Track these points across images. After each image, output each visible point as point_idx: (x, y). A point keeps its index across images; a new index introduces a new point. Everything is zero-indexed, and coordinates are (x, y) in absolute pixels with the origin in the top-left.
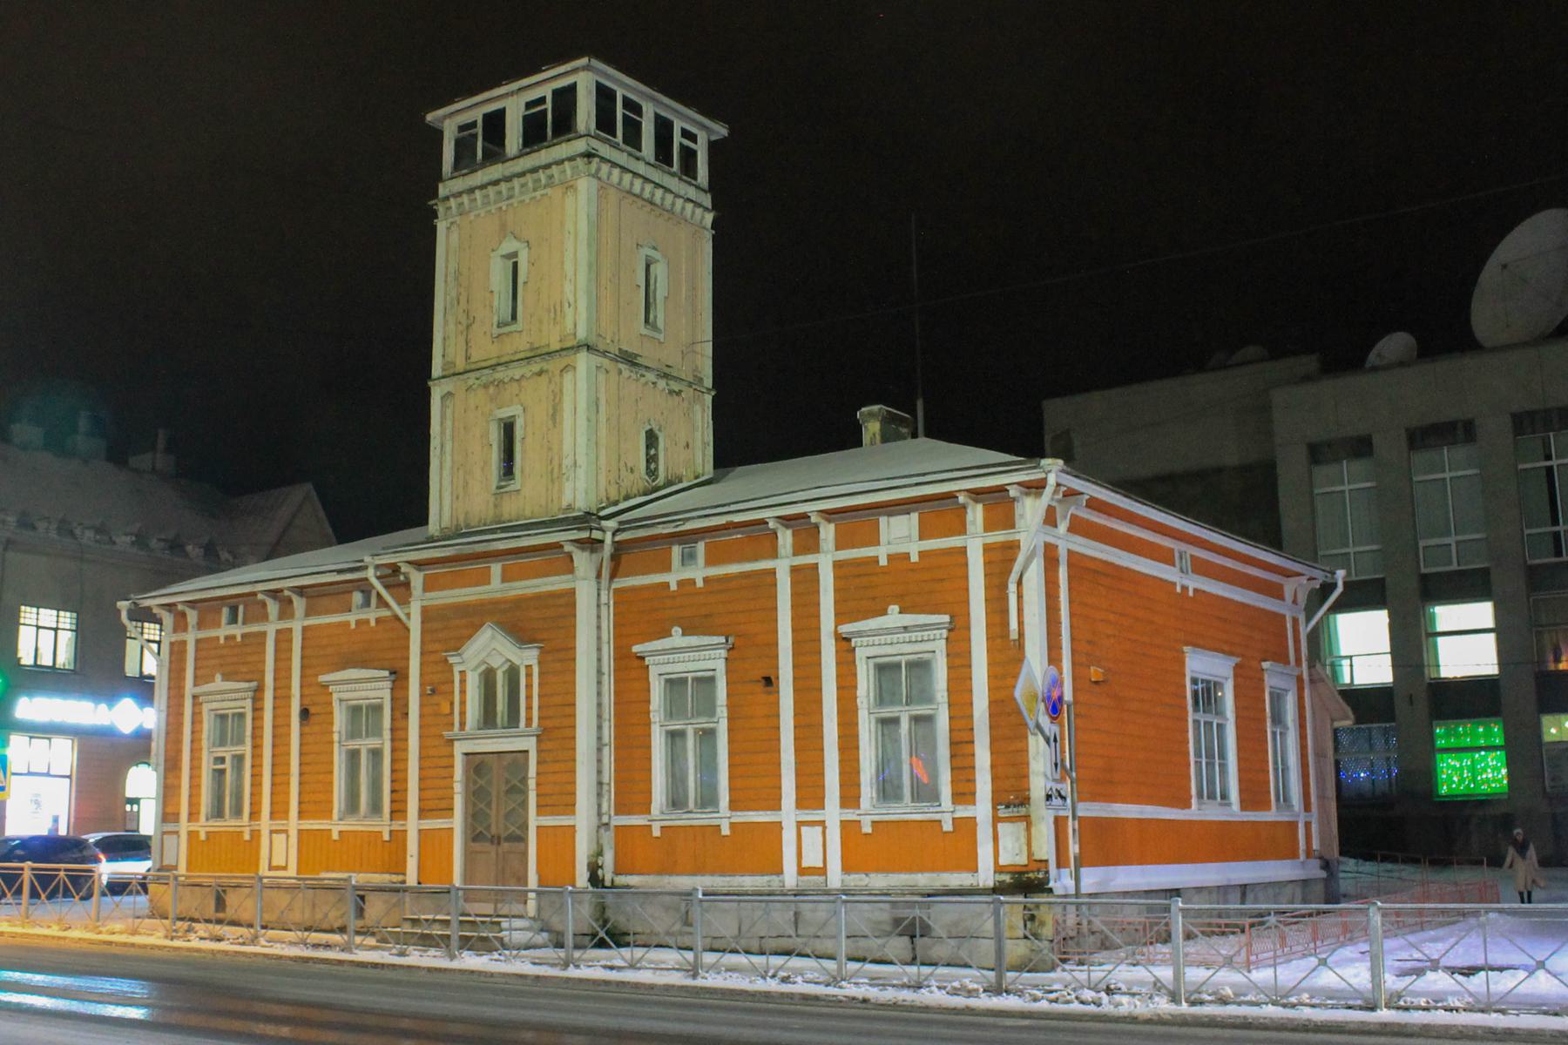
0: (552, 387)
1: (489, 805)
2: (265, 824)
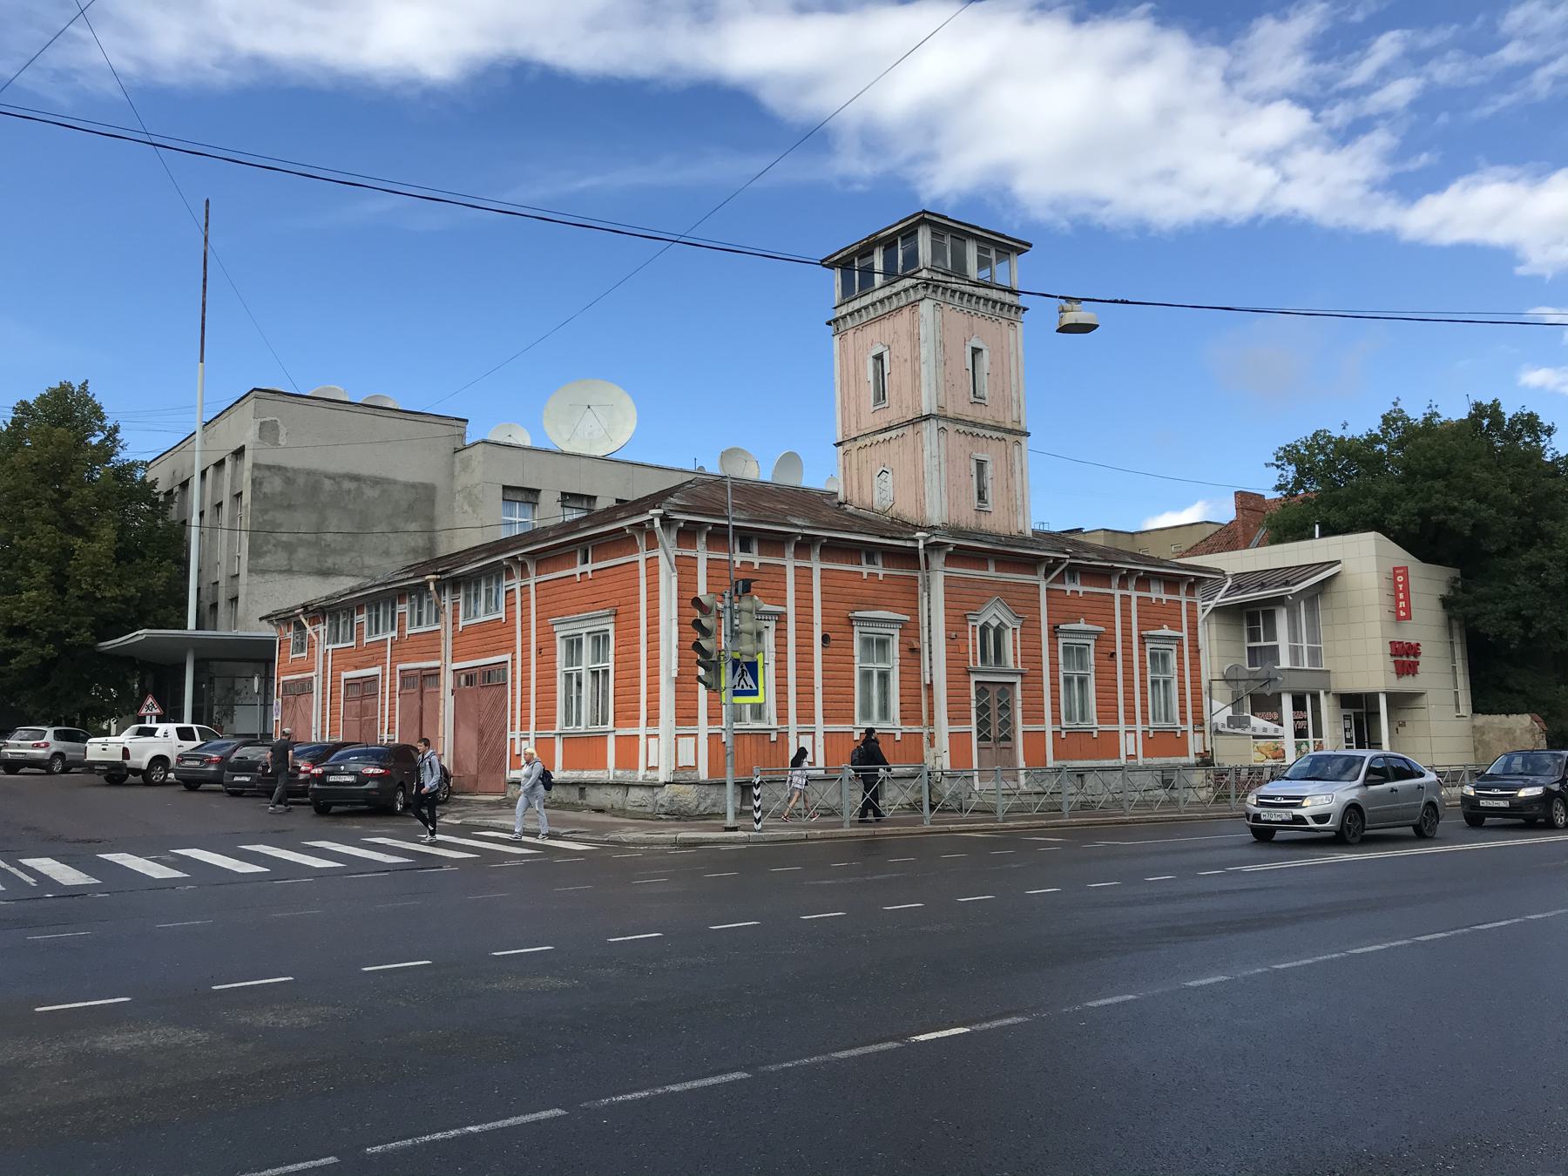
1: (988, 716)
2: (793, 725)
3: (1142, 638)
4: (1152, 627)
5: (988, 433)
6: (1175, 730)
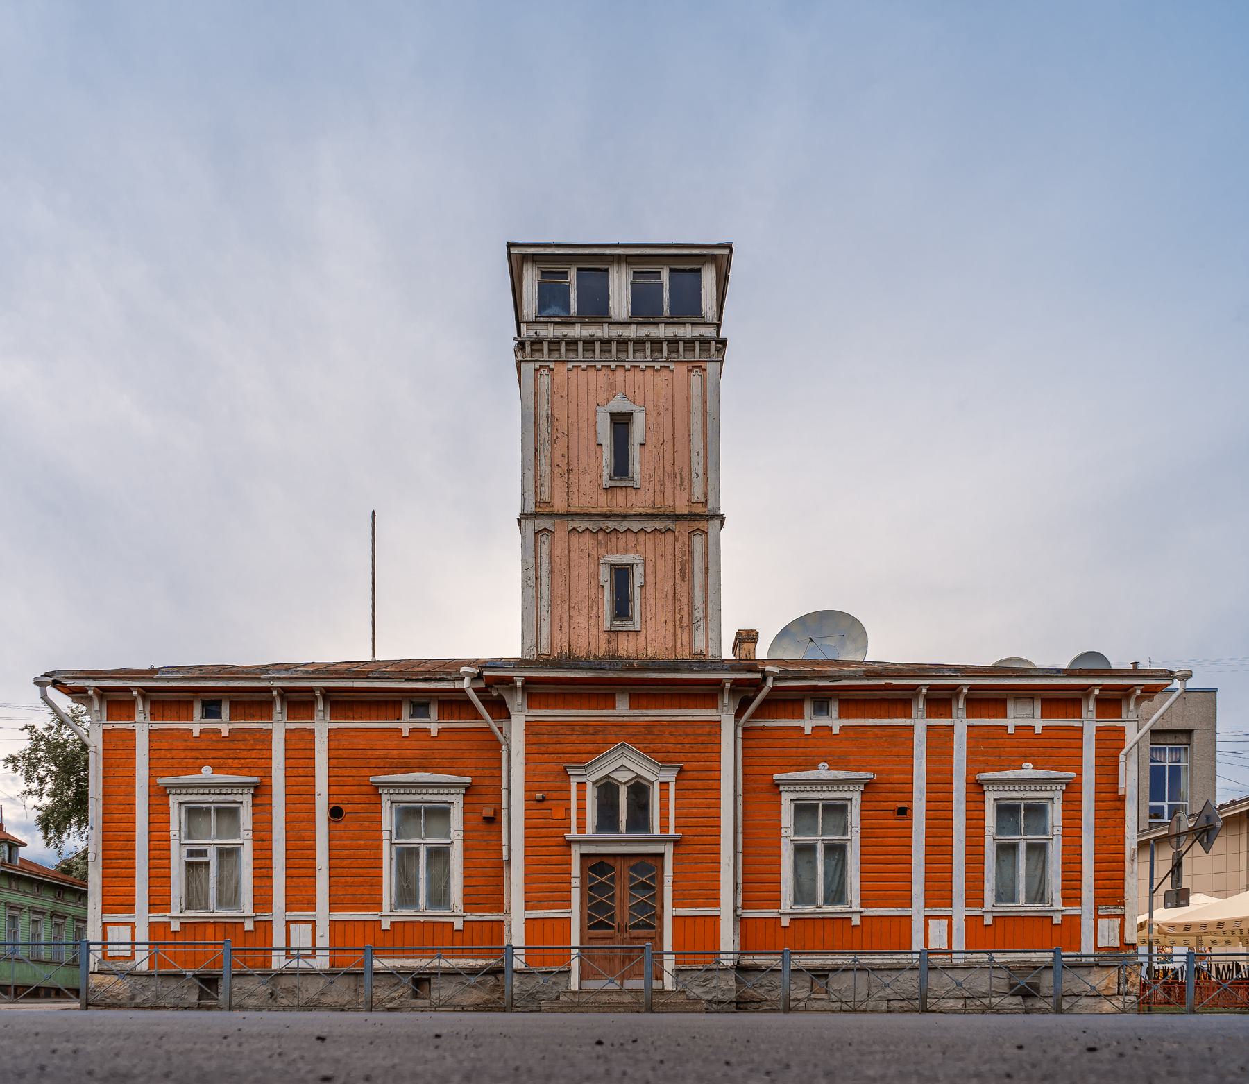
0: (679, 545)
3: (976, 789)
4: (1007, 767)
5: (636, 526)
6: (1049, 914)
